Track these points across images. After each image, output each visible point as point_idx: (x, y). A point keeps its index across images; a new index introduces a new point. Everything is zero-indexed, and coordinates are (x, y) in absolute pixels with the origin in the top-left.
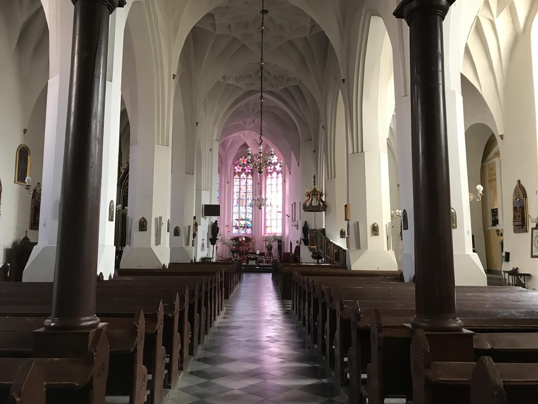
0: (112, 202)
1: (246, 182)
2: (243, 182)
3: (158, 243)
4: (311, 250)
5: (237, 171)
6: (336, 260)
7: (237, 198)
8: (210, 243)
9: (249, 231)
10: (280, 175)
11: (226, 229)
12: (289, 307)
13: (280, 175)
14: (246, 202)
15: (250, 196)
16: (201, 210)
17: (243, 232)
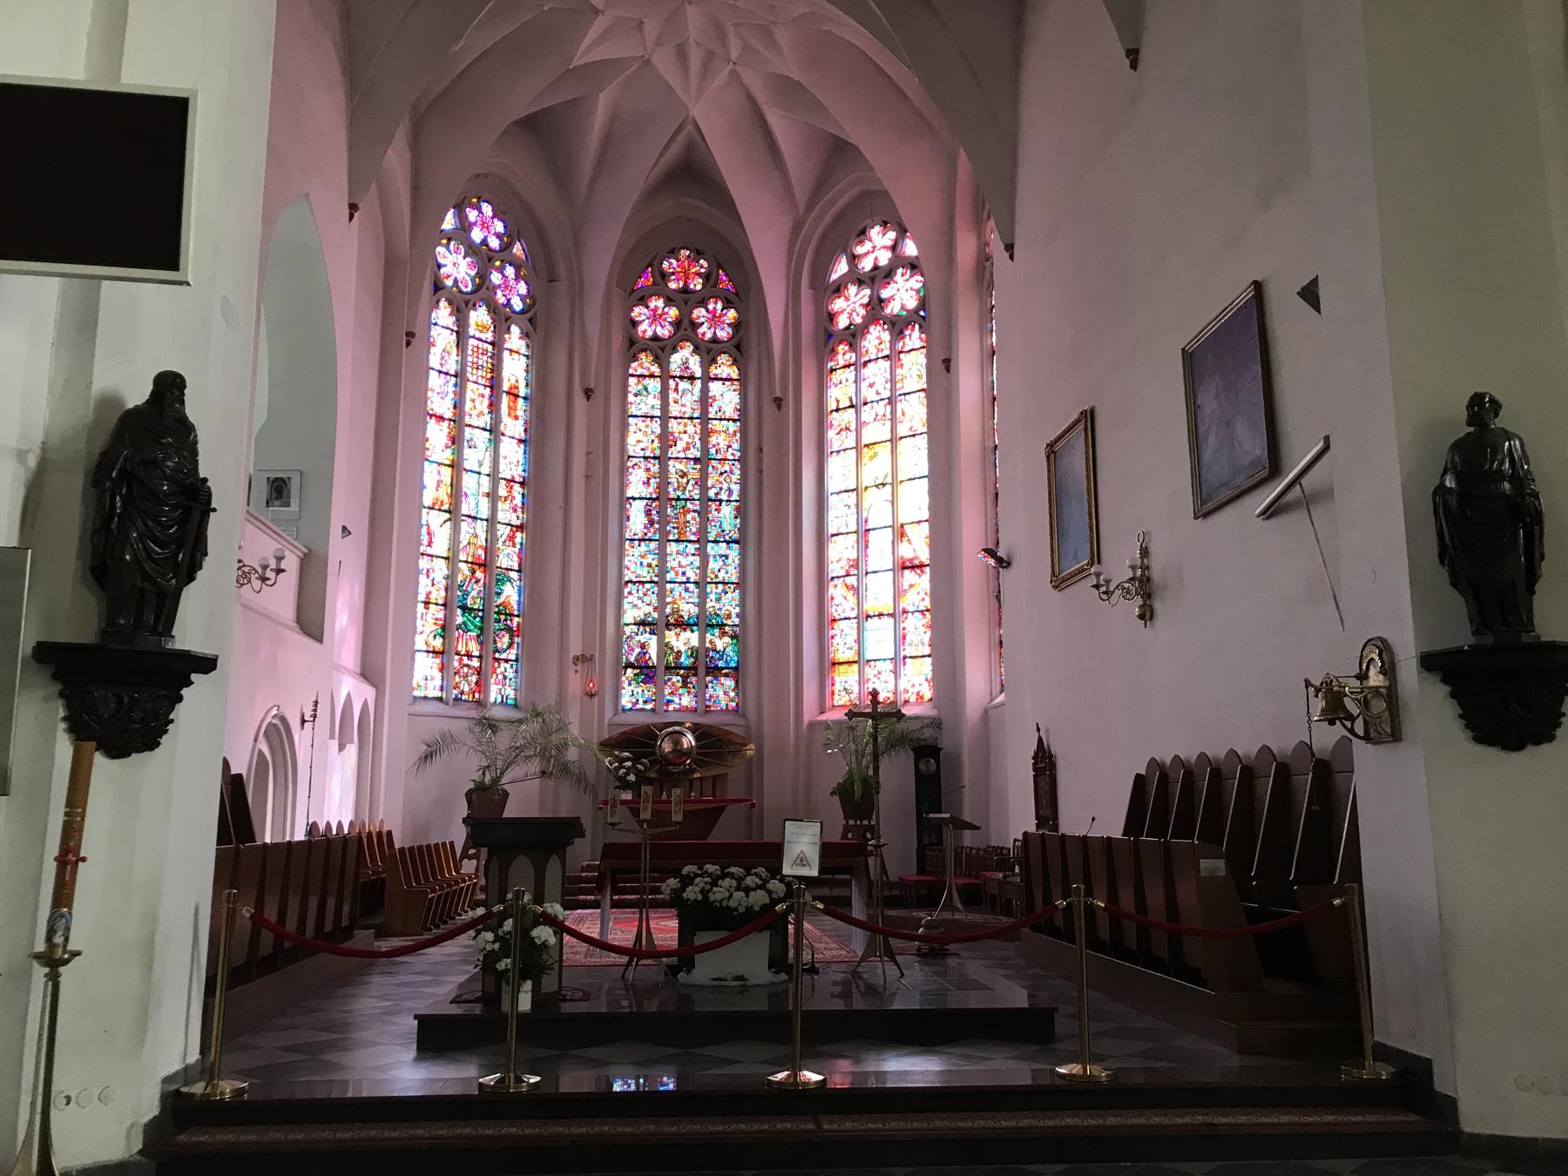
1: (705, 400)
2: (686, 399)
5: (646, 329)
7: (650, 491)
9: (722, 692)
10: (914, 338)
11: (575, 683)
13: (914, 338)
14: (703, 514)
15: (727, 482)
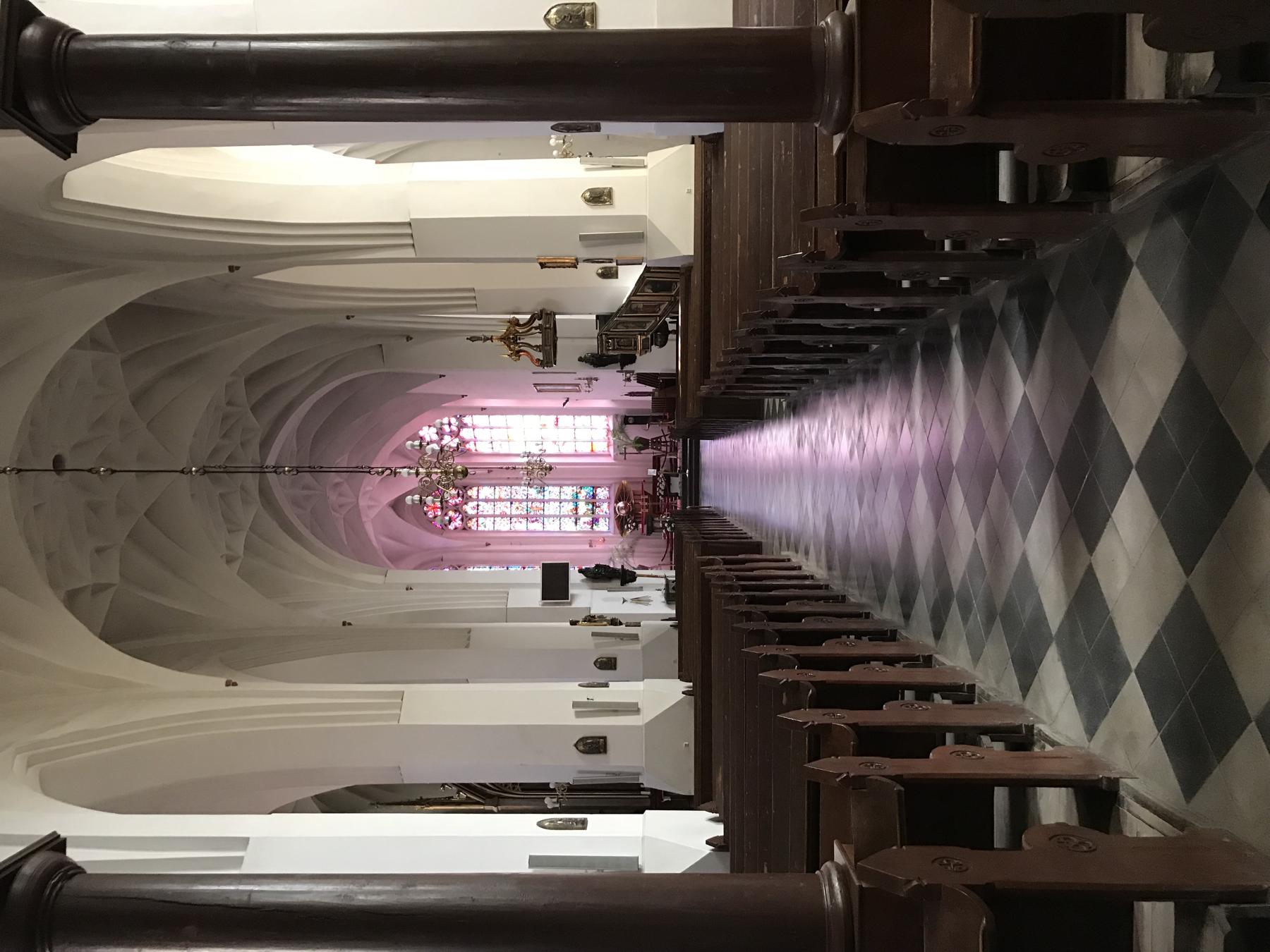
0: (540, 824)
1: (487, 500)
2: (486, 508)
3: (633, 709)
4: (646, 349)
5: (458, 523)
6: (670, 290)
7: (524, 521)
8: (631, 585)
9: (602, 493)
10: (467, 420)
12: (781, 404)
13: (467, 420)
15: (520, 492)
16: (556, 607)
17: (605, 506)
